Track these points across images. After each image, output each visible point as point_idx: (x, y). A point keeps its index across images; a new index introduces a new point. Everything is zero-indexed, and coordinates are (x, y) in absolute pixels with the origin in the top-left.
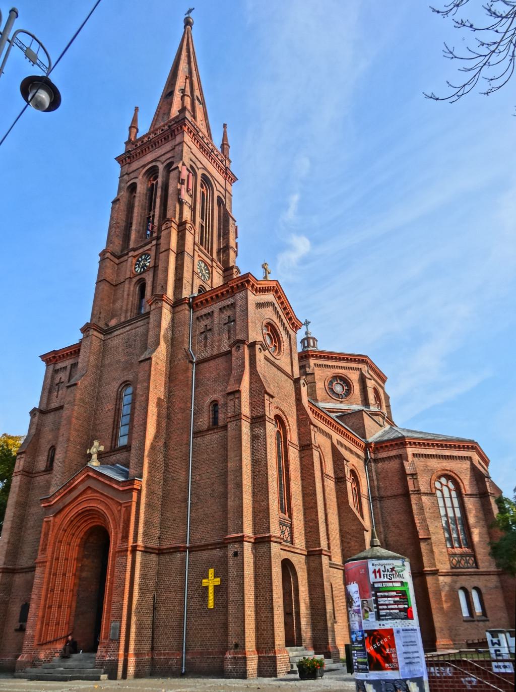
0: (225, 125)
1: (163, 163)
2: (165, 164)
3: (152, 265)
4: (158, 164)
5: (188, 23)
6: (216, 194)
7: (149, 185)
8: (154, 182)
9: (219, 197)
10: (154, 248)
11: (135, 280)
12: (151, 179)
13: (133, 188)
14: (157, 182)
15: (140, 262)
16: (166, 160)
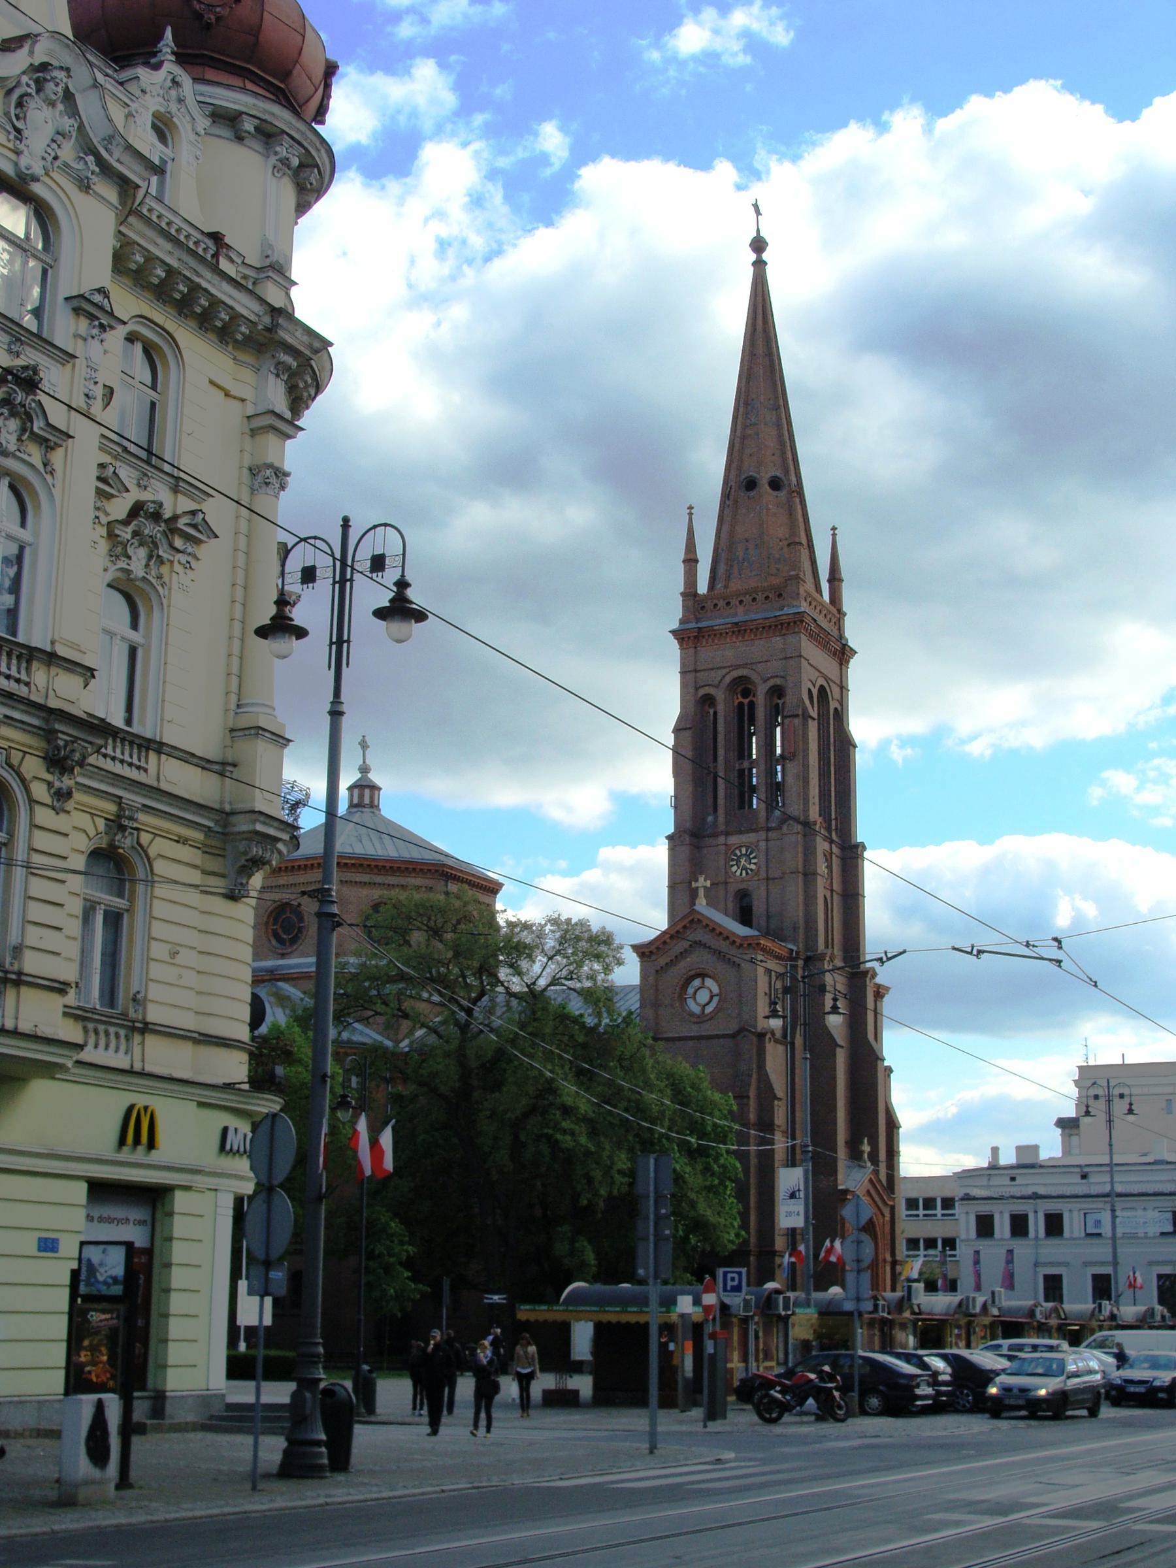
0: (834, 529)
1: (765, 681)
2: (771, 683)
3: (763, 875)
4: (754, 677)
5: (759, 245)
6: (833, 705)
7: (736, 703)
8: (746, 701)
9: (836, 709)
10: (762, 845)
11: (733, 888)
12: (739, 689)
13: (708, 701)
14: (752, 705)
15: (739, 857)
16: (769, 679)
